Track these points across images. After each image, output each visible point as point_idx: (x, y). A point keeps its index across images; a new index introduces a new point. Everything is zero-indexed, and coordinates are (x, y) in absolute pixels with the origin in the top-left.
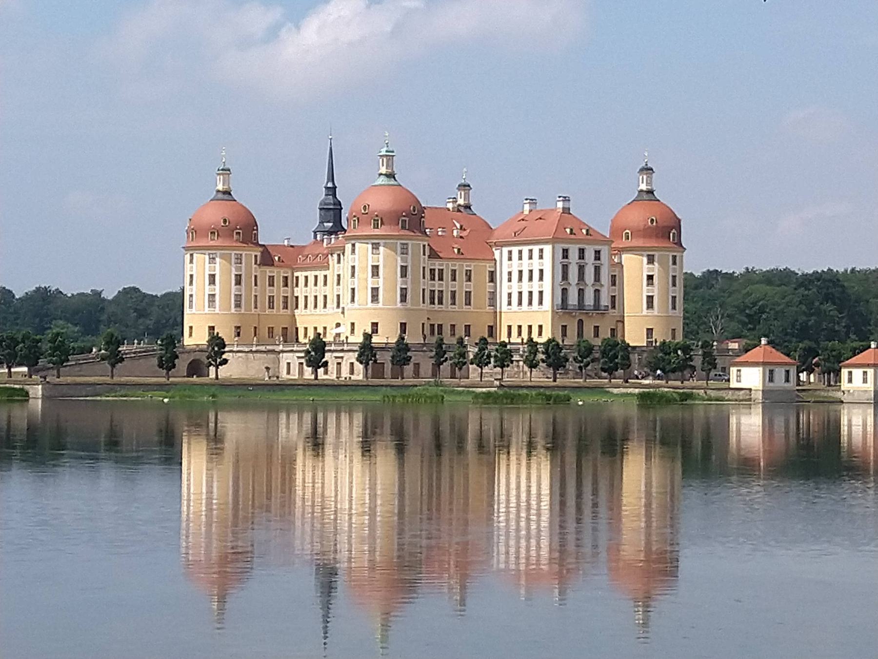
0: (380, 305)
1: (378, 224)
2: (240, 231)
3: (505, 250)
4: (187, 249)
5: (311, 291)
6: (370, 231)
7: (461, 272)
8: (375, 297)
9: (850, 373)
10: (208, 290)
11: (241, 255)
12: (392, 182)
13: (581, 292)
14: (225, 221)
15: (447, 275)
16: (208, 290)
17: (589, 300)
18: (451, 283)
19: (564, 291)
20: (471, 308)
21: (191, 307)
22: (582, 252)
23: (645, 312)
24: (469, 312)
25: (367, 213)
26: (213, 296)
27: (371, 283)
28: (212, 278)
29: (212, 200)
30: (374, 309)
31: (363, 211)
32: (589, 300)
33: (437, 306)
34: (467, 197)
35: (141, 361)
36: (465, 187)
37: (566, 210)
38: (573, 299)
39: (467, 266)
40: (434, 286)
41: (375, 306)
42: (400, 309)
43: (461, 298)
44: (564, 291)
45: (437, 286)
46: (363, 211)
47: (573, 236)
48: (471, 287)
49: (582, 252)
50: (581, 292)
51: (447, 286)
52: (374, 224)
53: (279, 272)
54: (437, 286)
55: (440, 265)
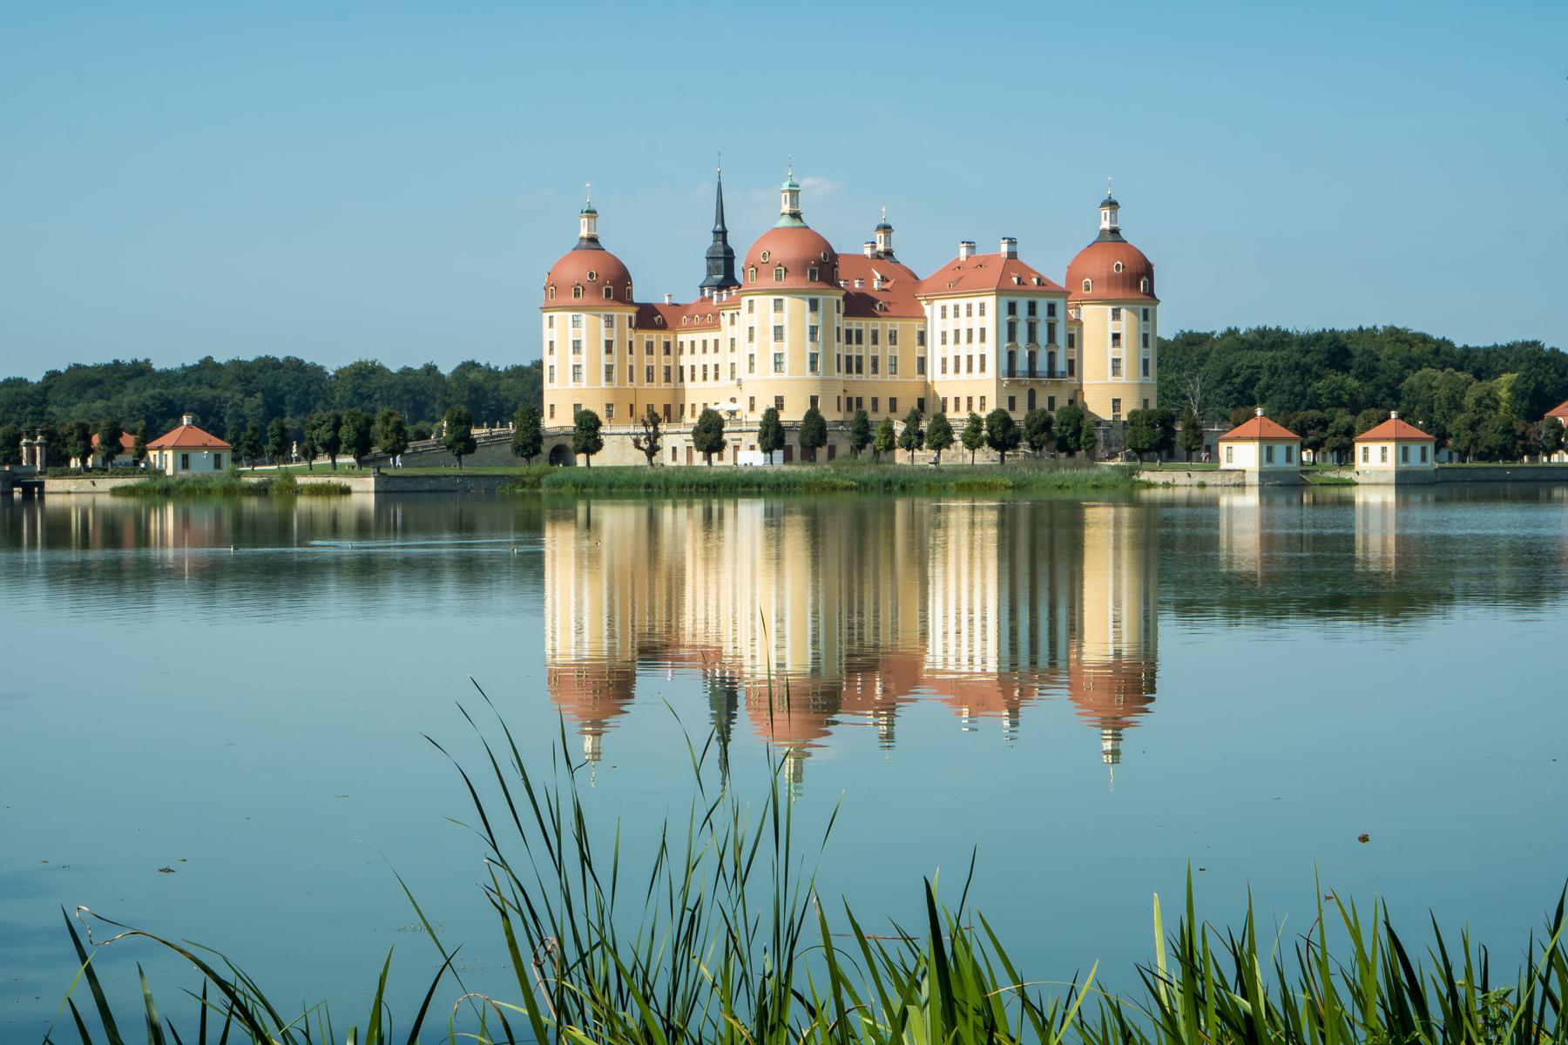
0: (786, 375)
1: (781, 275)
2: (611, 287)
3: (938, 304)
4: (545, 309)
5: (699, 359)
6: (771, 282)
9: (1366, 449)
10: (572, 359)
11: (612, 316)
12: (797, 223)
13: (1032, 356)
14: (591, 275)
15: (867, 337)
16: (572, 359)
17: (1042, 365)
18: (871, 347)
20: (898, 377)
21: (551, 380)
22: (1032, 307)
23: (1110, 378)
25: (767, 262)
26: (577, 367)
27: (773, 347)
28: (577, 346)
29: (574, 249)
30: (779, 380)
31: (762, 260)
32: (1042, 365)
33: (854, 376)
34: (888, 242)
35: (493, 448)
36: (886, 229)
37: (1012, 255)
38: (1022, 365)
40: (851, 350)
41: (779, 376)
43: (883, 365)
45: (854, 350)
46: (762, 260)
47: (1021, 287)
49: (1032, 307)
51: (866, 350)
52: (776, 275)
53: (659, 337)
54: (854, 350)
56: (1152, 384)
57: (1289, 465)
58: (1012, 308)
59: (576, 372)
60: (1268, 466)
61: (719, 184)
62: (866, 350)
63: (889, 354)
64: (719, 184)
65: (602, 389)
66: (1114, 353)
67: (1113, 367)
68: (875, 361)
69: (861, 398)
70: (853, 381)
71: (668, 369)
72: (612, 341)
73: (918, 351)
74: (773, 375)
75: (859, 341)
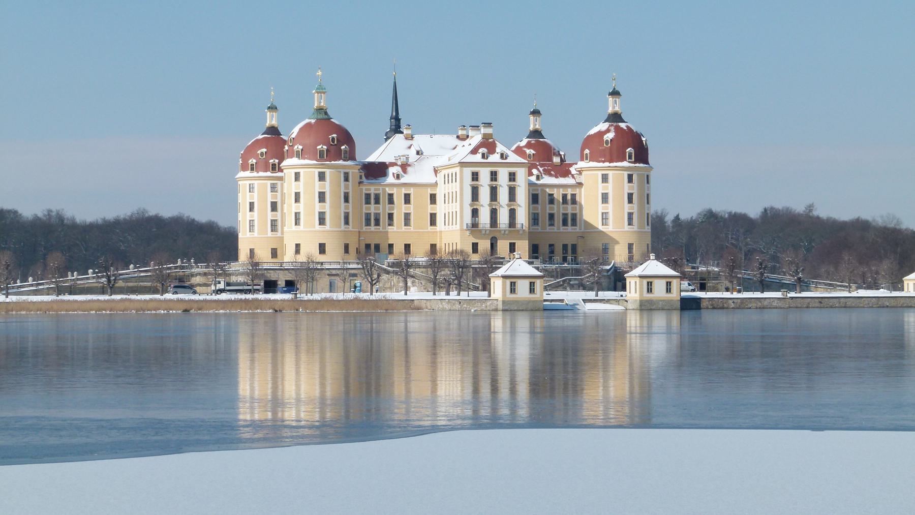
7: (384, 196)
8: (322, 221)
9: (908, 284)
13: (494, 213)
15: (384, 199)
17: (503, 218)
18: (364, 206)
19: (475, 213)
20: (411, 229)
22: (494, 176)
24: (378, 232)
32: (503, 218)
33: (373, 228)
38: (484, 218)
39: (366, 190)
40: (370, 209)
42: (319, 232)
43: (384, 219)
44: (475, 213)
45: (372, 208)
48: (411, 208)
49: (494, 176)
50: (494, 213)
51: (383, 209)
54: (372, 208)
55: (375, 190)
56: (648, 232)
57: (532, 296)
58: (475, 176)
59: (604, 217)
60: (510, 296)
61: (395, 83)
62: (383, 209)
63: (364, 211)
64: (395, 83)
65: (268, 237)
66: (603, 208)
67: (272, 225)
68: (391, 216)
69: (379, 244)
70: (372, 232)
71: (565, 215)
72: (253, 203)
73: (430, 209)
74: (318, 227)
75: (377, 201)
